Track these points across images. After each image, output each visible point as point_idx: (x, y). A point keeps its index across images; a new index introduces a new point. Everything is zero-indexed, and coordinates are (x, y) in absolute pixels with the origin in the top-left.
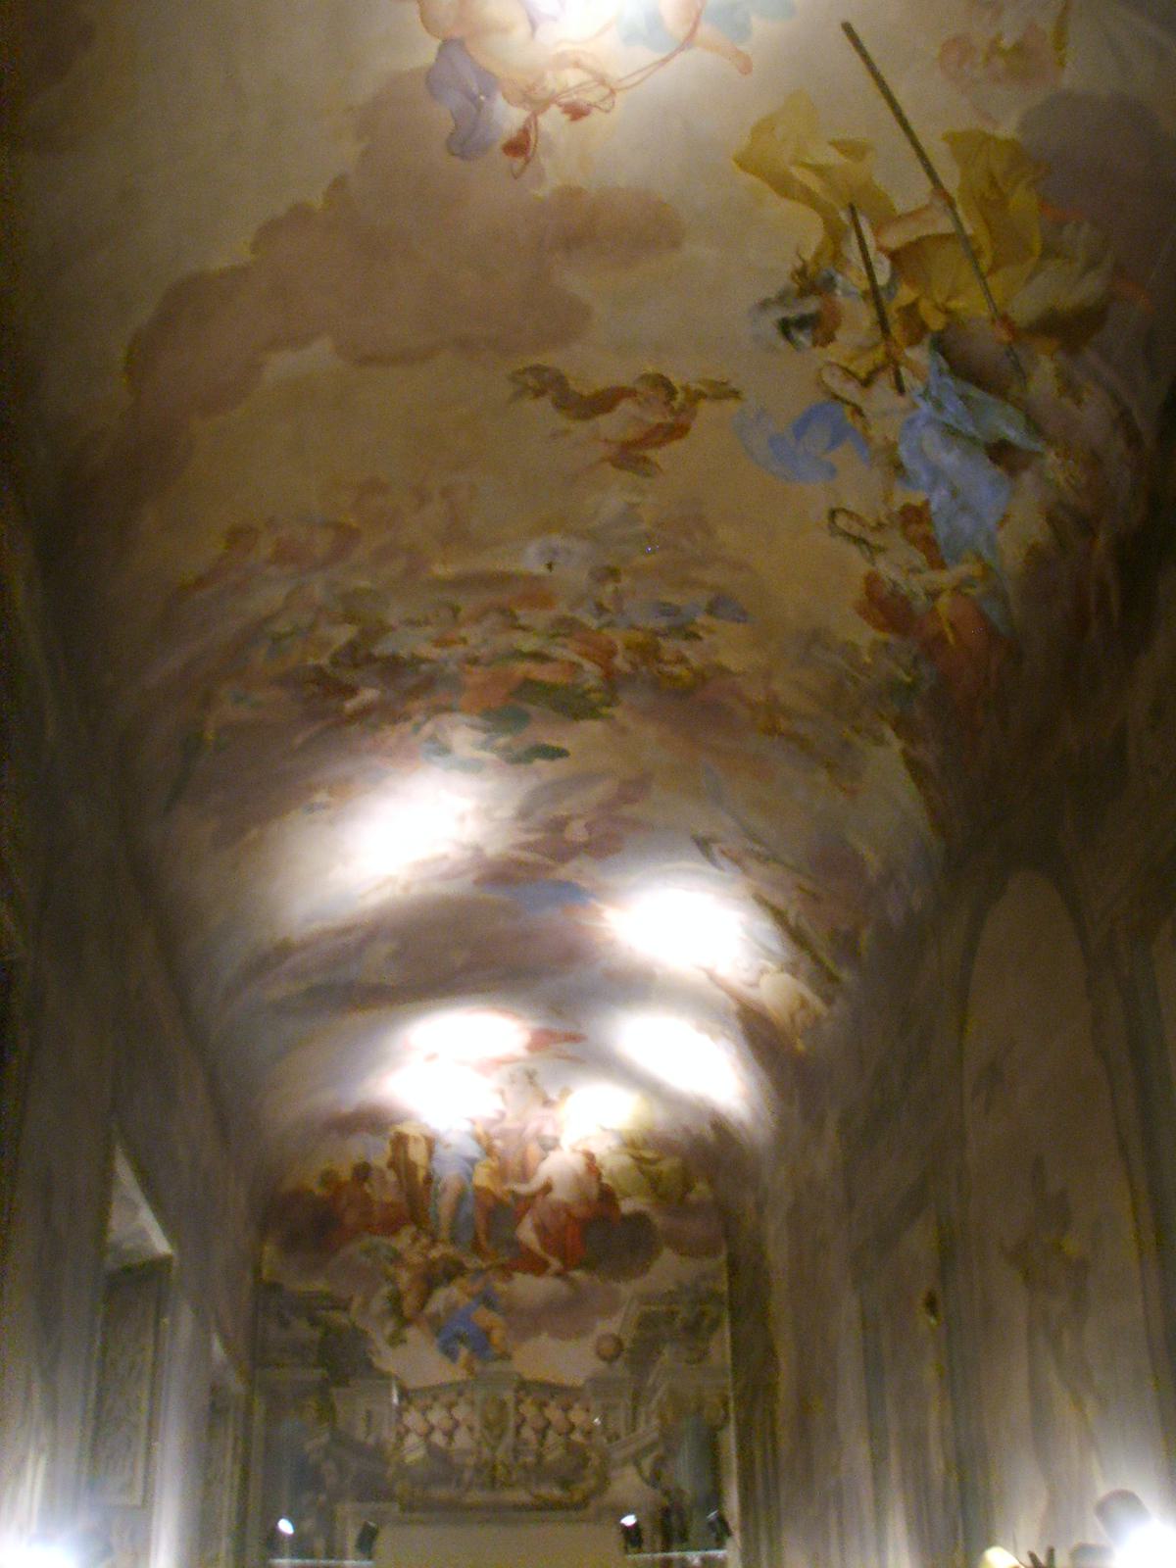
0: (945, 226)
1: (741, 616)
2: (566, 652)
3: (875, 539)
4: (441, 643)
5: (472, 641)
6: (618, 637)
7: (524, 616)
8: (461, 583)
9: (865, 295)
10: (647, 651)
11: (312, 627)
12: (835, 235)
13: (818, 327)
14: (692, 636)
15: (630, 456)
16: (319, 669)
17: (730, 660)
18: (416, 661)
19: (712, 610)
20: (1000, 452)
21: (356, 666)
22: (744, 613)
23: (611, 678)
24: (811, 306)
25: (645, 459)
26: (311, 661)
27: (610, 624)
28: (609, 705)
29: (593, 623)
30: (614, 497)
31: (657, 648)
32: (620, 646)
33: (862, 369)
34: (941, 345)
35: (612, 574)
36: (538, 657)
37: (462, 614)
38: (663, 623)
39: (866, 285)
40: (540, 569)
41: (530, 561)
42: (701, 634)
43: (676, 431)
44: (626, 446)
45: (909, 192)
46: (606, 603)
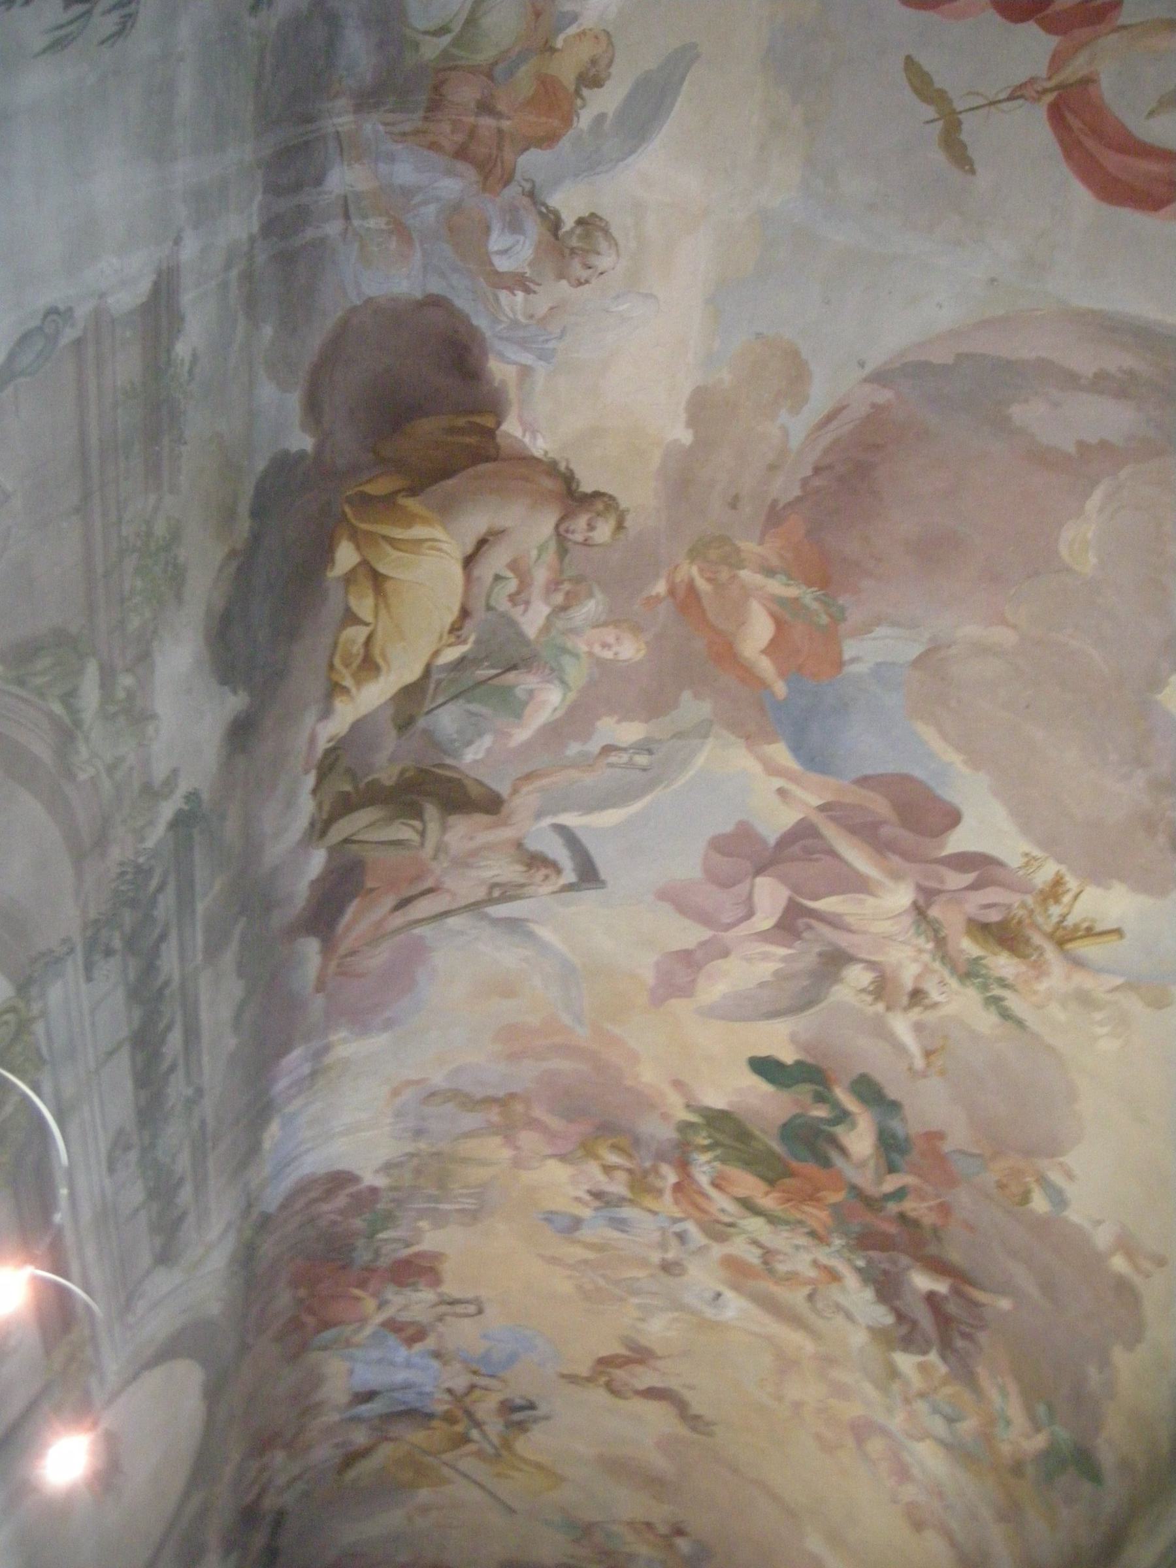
0: (446, 1457)
1: (550, 1217)
2: (721, 1203)
3: (444, 1308)
4: (834, 1276)
5: (808, 1258)
6: (667, 1204)
7: (753, 1256)
8: (794, 1319)
9: (484, 1423)
10: (642, 1184)
11: (922, 1395)
12: (507, 1444)
13: (508, 1408)
14: (597, 1195)
15: (640, 1355)
16: (944, 1358)
17: (558, 1172)
18: (867, 1276)
19: (577, 1223)
20: (369, 1396)
21: (914, 1324)
22: (546, 1219)
23: (683, 1165)
24: (517, 1416)
25: (631, 1349)
26: (943, 1369)
27: (675, 1221)
28: (690, 1125)
29: (691, 1227)
30: (658, 1329)
31: (632, 1187)
32: (668, 1197)
33: (477, 1393)
34: (430, 1416)
35: (667, 1267)
36: (748, 1206)
37: (806, 1290)
38: (627, 1212)
39: (486, 1428)
40: (729, 1294)
41: (735, 1306)
42: (588, 1198)
43: (605, 1362)
44: (641, 1362)
45: (468, 1464)
46: (674, 1242)
